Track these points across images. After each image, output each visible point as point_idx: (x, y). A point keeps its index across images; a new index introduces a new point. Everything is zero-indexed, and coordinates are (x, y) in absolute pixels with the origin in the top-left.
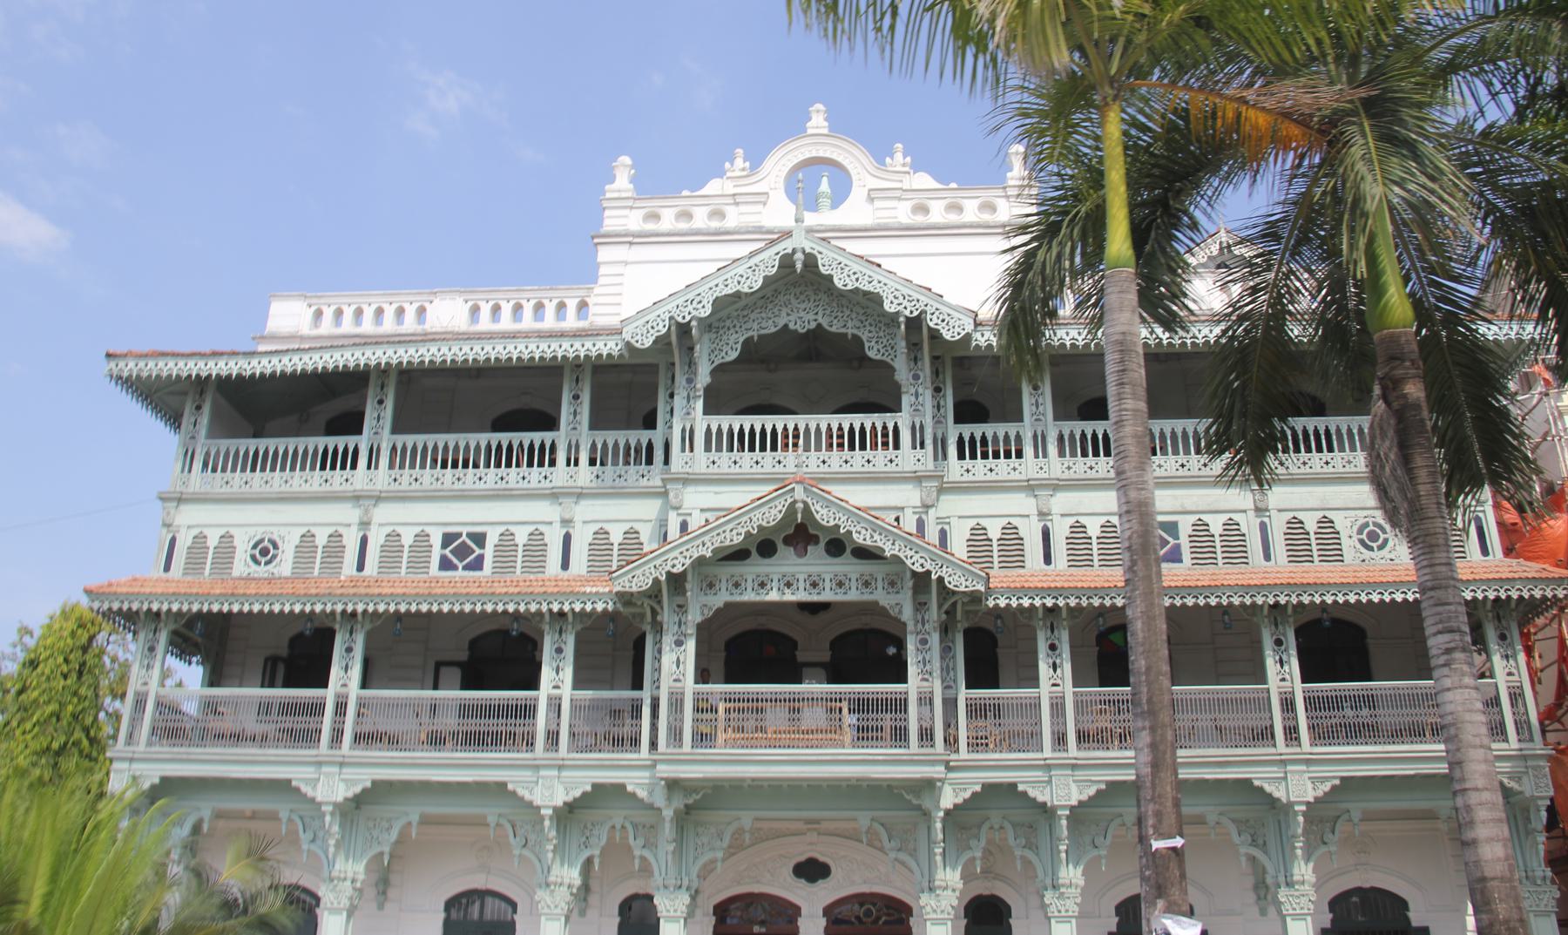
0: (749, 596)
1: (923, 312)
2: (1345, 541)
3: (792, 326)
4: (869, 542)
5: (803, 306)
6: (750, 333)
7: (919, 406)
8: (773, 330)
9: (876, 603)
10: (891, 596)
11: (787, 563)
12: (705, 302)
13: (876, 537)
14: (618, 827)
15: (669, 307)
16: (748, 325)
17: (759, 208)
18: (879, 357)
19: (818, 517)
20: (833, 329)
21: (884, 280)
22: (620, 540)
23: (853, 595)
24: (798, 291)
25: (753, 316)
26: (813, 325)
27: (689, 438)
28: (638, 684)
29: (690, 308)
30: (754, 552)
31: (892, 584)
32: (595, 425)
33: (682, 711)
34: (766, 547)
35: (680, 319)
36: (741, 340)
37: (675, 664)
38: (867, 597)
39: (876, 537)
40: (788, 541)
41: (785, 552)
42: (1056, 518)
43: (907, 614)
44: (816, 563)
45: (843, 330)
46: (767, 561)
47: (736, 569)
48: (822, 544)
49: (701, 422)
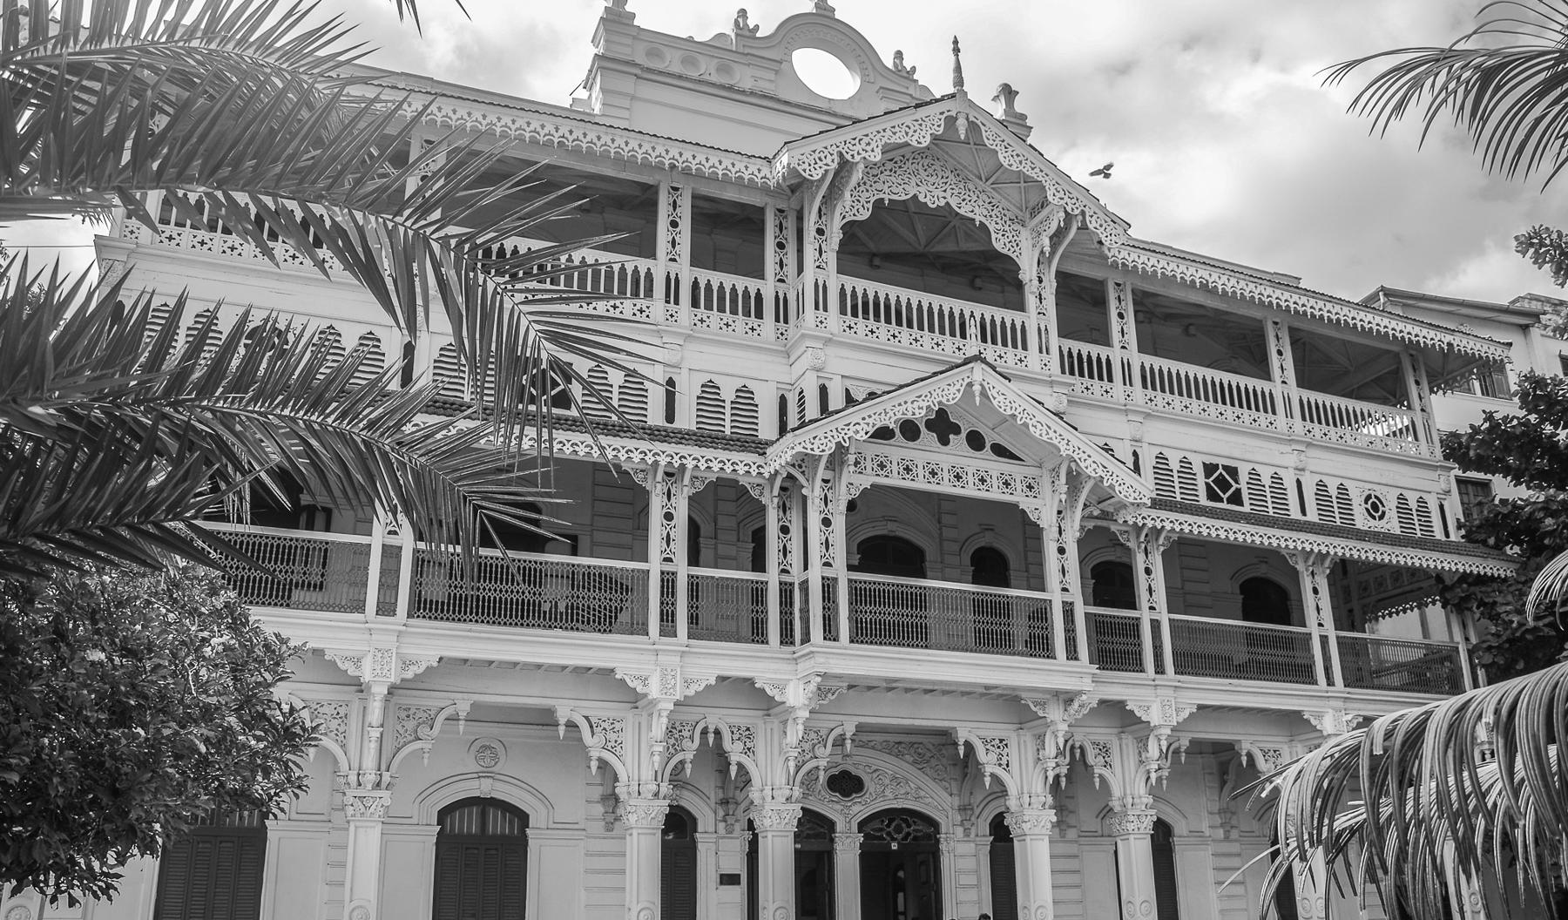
0: (895, 481)
1: (1083, 213)
2: (1355, 506)
3: (921, 198)
4: (1045, 438)
5: (932, 180)
6: (881, 196)
7: (1040, 311)
8: (904, 198)
9: (1013, 508)
10: (1030, 499)
11: (927, 451)
12: (873, 145)
13: (1052, 434)
14: (711, 729)
15: (837, 141)
16: (879, 186)
17: (772, 76)
18: (1005, 251)
19: (995, 403)
20: (962, 212)
21: (1046, 170)
22: (733, 398)
23: (996, 494)
24: (926, 162)
25: (882, 177)
26: (942, 203)
27: (821, 291)
28: (759, 564)
29: (858, 148)
30: (897, 431)
31: (1030, 487)
32: (696, 261)
33: (791, 604)
34: (910, 430)
35: (848, 157)
36: (873, 200)
37: (815, 550)
38: (1007, 498)
39: (1052, 434)
40: (930, 425)
41: (928, 438)
42: (1145, 445)
43: (1046, 518)
44: (957, 453)
45: (971, 215)
46: (911, 444)
47: (882, 448)
48: (964, 435)
49: (834, 281)
